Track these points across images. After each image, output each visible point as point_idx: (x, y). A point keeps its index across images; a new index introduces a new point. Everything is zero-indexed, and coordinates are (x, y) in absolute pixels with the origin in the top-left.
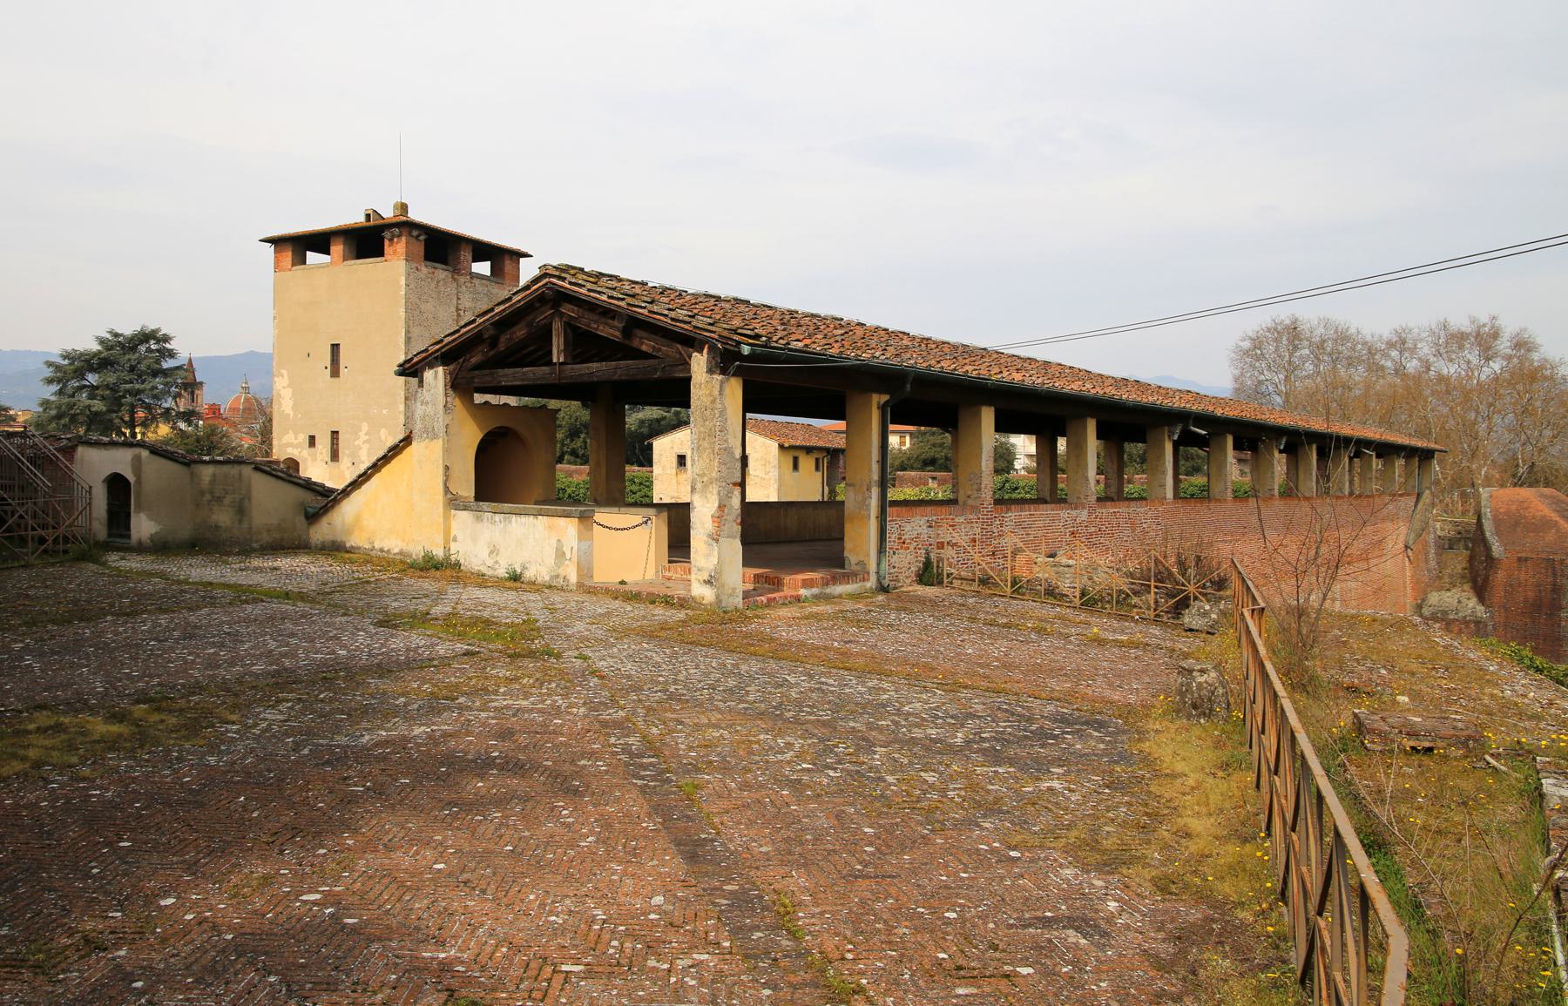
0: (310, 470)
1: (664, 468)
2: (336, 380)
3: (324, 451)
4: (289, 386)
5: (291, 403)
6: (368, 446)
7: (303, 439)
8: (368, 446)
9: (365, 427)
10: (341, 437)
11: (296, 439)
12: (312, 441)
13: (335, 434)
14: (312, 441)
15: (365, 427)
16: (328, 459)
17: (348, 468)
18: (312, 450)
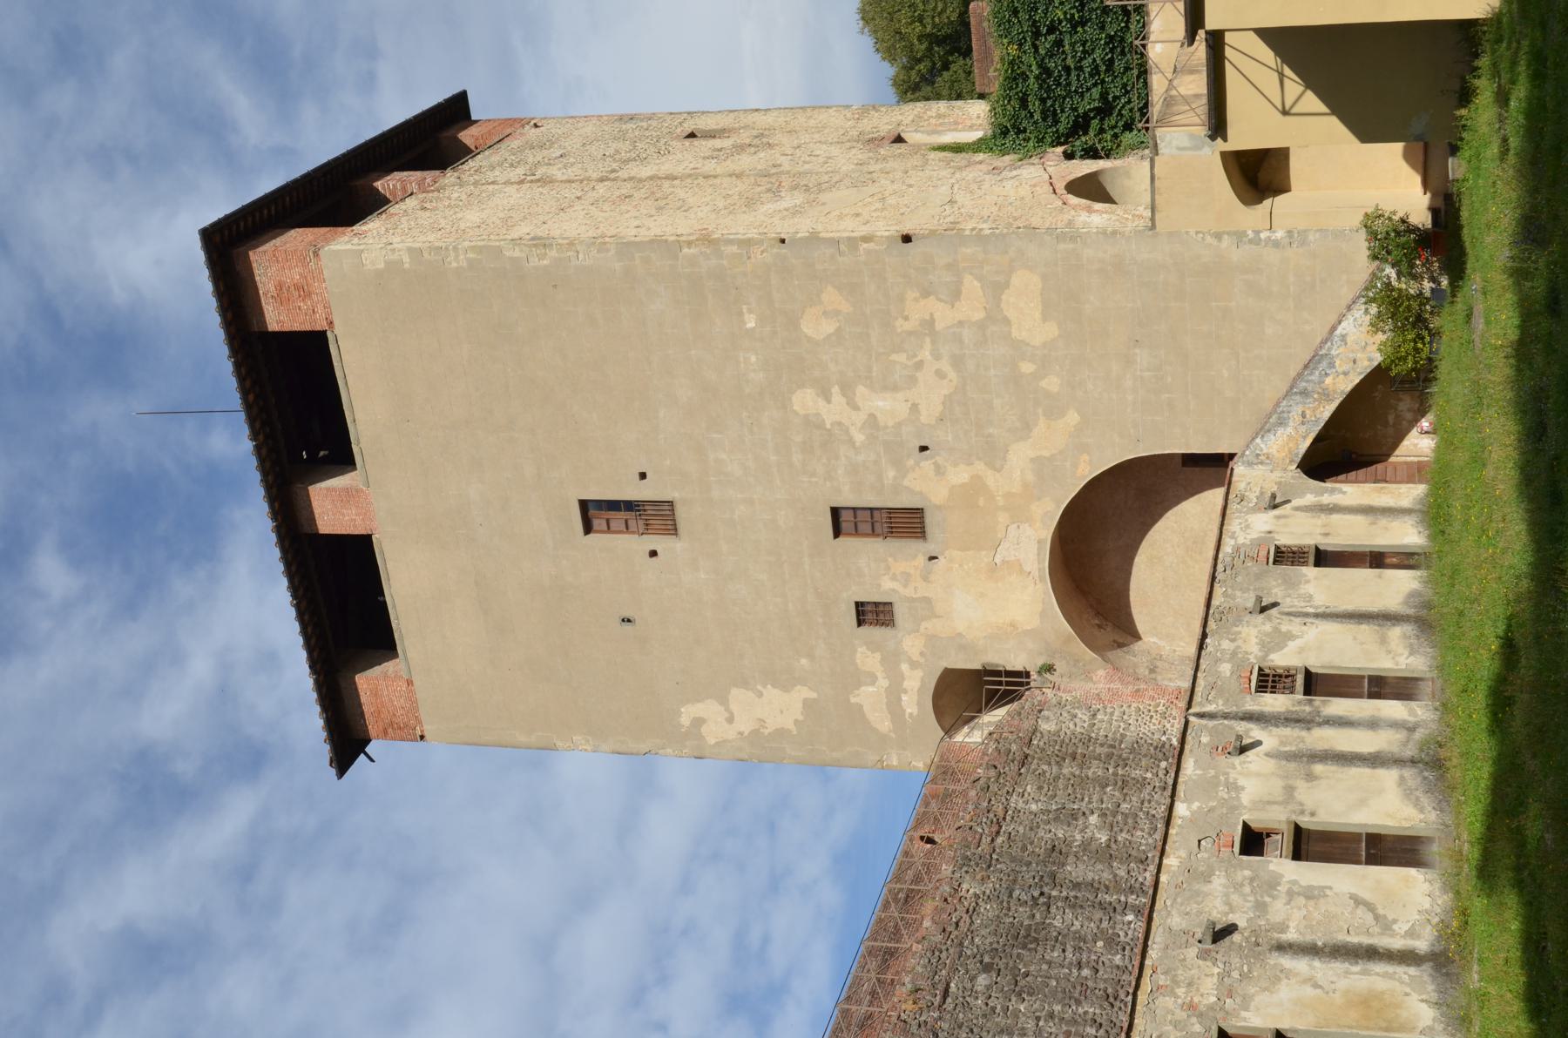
4: (724, 701)
5: (771, 692)
6: (861, 390)
7: (866, 648)
8: (861, 390)
9: (805, 401)
10: (847, 499)
11: (873, 679)
12: (871, 614)
14: (871, 614)
17: (939, 471)
18: (900, 612)
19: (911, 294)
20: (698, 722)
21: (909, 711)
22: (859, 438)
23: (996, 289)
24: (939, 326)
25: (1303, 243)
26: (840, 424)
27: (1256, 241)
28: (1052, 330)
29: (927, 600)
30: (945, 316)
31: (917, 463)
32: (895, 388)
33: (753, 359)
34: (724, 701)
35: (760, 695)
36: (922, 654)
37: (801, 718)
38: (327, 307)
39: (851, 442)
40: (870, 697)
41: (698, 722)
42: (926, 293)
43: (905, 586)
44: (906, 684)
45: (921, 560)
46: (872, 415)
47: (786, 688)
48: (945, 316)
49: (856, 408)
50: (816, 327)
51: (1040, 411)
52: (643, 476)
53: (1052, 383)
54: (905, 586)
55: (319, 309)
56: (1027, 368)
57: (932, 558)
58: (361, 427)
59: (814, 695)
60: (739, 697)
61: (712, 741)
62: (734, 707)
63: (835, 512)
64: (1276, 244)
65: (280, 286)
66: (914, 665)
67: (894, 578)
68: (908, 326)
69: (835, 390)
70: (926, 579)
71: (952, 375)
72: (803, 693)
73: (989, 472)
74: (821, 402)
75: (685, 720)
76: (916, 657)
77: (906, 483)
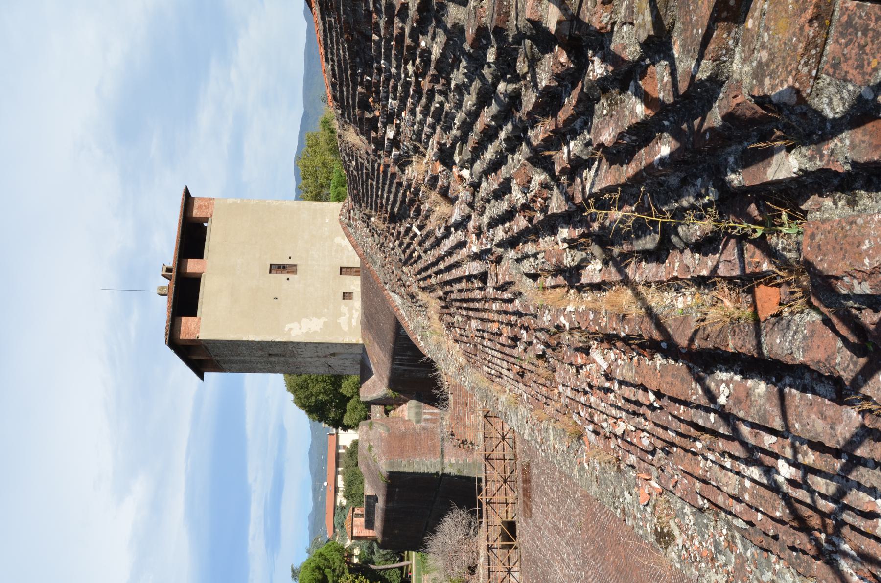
2: (299, 268)
4: (299, 323)
5: (314, 319)
7: (344, 306)
13: (344, 271)
20: (291, 329)
34: (299, 323)
38: (212, 212)
40: (343, 321)
41: (291, 329)
47: (319, 318)
52: (290, 258)
55: (210, 212)
58: (211, 242)
60: (305, 321)
61: (293, 335)
63: (341, 268)
65: (200, 206)
66: (357, 310)
72: (324, 319)
75: (286, 329)
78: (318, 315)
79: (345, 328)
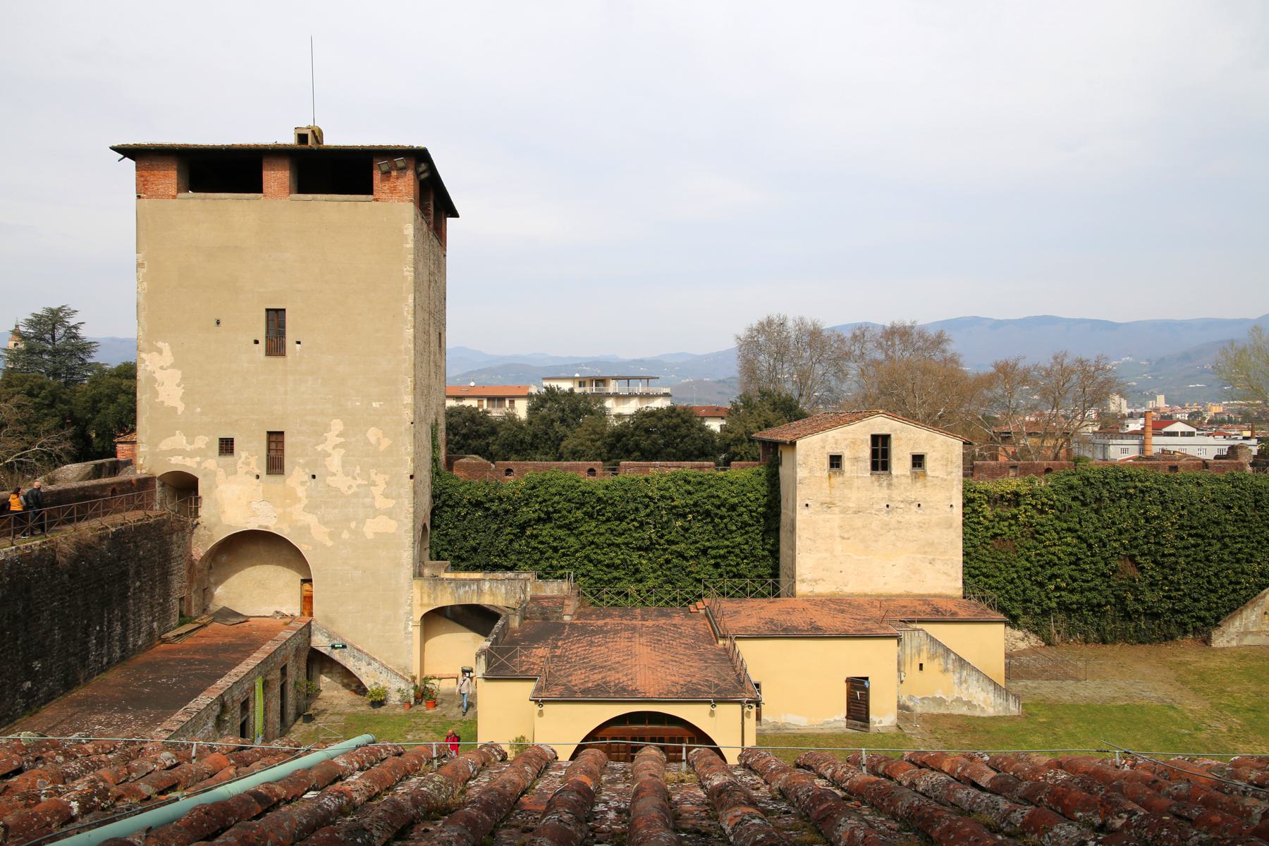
0: (222, 487)
1: (811, 470)
2: (279, 359)
3: (253, 461)
4: (173, 366)
5: (180, 391)
6: (343, 451)
7: (207, 442)
8: (343, 451)
9: (337, 425)
10: (288, 440)
12: (227, 446)
13: (275, 438)
14: (227, 446)
15: (337, 425)
16: (262, 471)
17: (303, 483)
18: (227, 459)
19: (387, 477)
20: (160, 352)
21: (173, 459)
22: (319, 448)
23: (389, 513)
24: (372, 488)
25: (407, 638)
26: (326, 440)
27: (408, 619)
28: (370, 536)
29: (235, 473)
30: (377, 491)
31: (306, 474)
32: (343, 467)
33: (358, 404)
34: (173, 366)
35: (178, 385)
36: (206, 468)
37: (166, 404)
39: (317, 444)
40: (179, 440)
41: (160, 352)
42: (387, 483)
43: (243, 463)
44: (188, 459)
45: (258, 472)
46: (330, 455)
47: (182, 399)
48: (377, 491)
49: (334, 448)
50: (373, 434)
51: (333, 529)
53: (346, 535)
54: (243, 463)
56: (353, 525)
57: (258, 477)
59: (179, 412)
60: (178, 374)
62: (170, 371)
64: (406, 628)
66: (199, 464)
67: (247, 458)
68: (373, 475)
69: (342, 440)
70: (247, 473)
71: (350, 492)
72: (181, 408)
73: (303, 506)
74: (337, 433)
75: (160, 344)
76: (204, 465)
77: (297, 468)
78: (187, 397)
79: (165, 445)
